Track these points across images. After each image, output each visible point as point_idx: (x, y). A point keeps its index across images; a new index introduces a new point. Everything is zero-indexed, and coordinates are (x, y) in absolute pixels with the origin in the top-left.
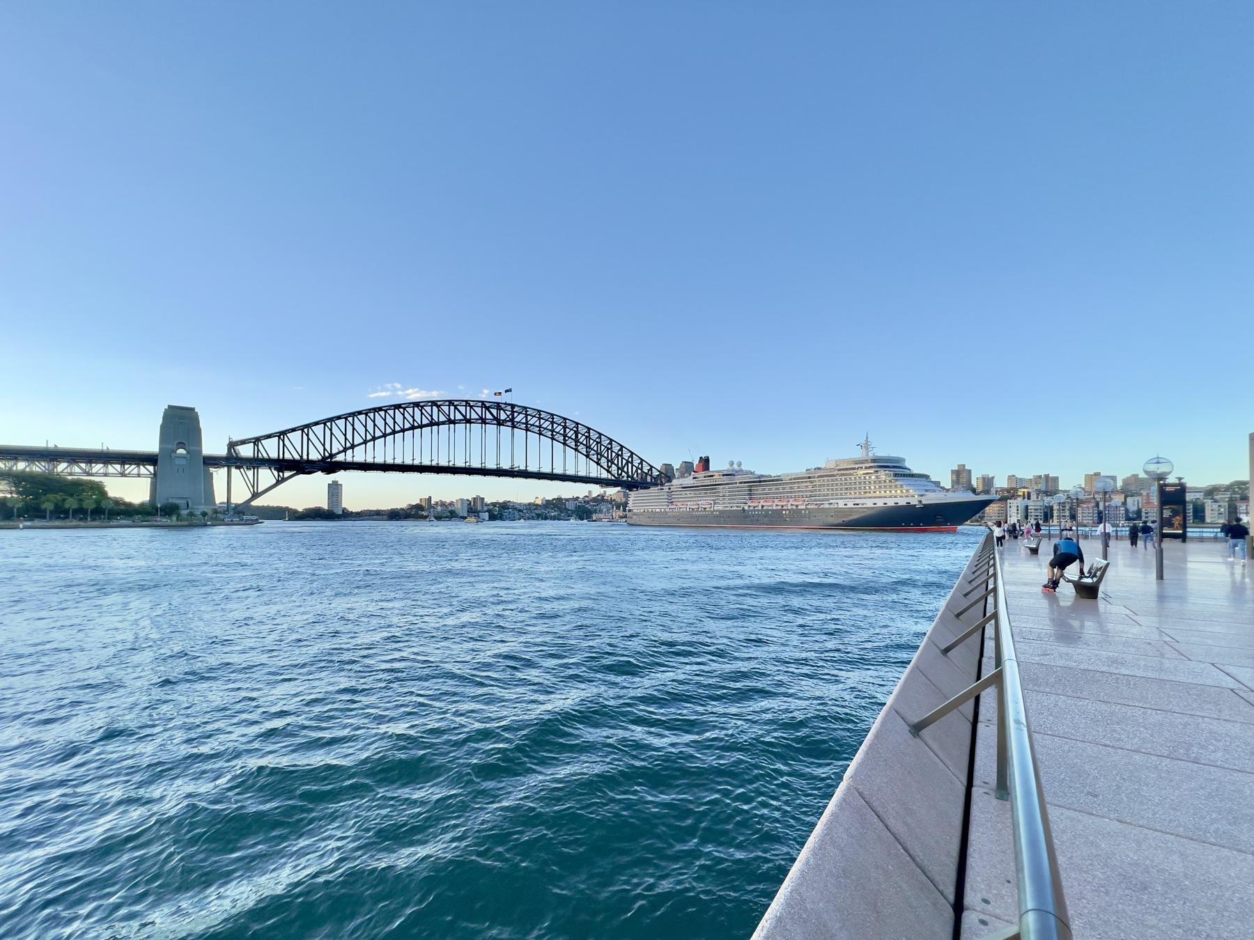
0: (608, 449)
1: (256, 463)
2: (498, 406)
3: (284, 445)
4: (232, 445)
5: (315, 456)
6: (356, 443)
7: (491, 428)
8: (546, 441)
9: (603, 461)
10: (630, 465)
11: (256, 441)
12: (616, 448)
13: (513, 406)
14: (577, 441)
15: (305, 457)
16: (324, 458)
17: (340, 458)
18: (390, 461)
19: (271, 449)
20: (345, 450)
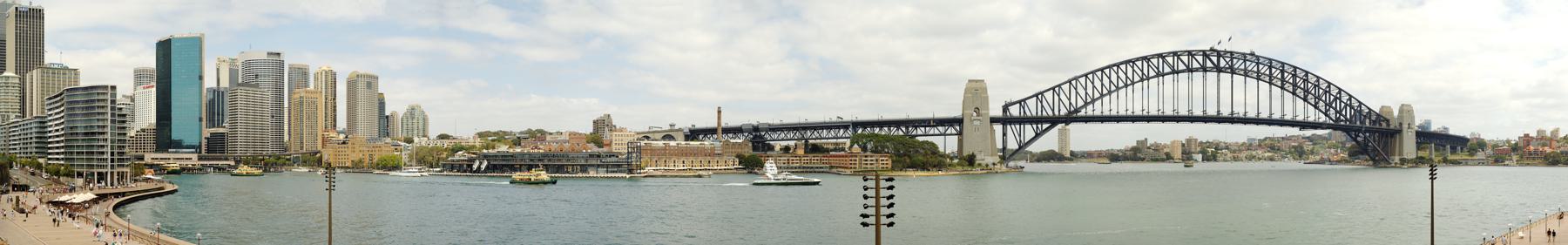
0: (1326, 92)
1: (1022, 121)
2: (1219, 54)
3: (1042, 106)
4: (1006, 108)
5: (1064, 112)
6: (1095, 97)
7: (1212, 76)
8: (1264, 86)
9: (1321, 104)
10: (1348, 108)
11: (1022, 102)
12: (1334, 92)
13: (1231, 53)
14: (1295, 85)
15: (1057, 113)
16: (1070, 112)
17: (1082, 113)
18: (1122, 113)
19: (1032, 108)
20: (1086, 104)
